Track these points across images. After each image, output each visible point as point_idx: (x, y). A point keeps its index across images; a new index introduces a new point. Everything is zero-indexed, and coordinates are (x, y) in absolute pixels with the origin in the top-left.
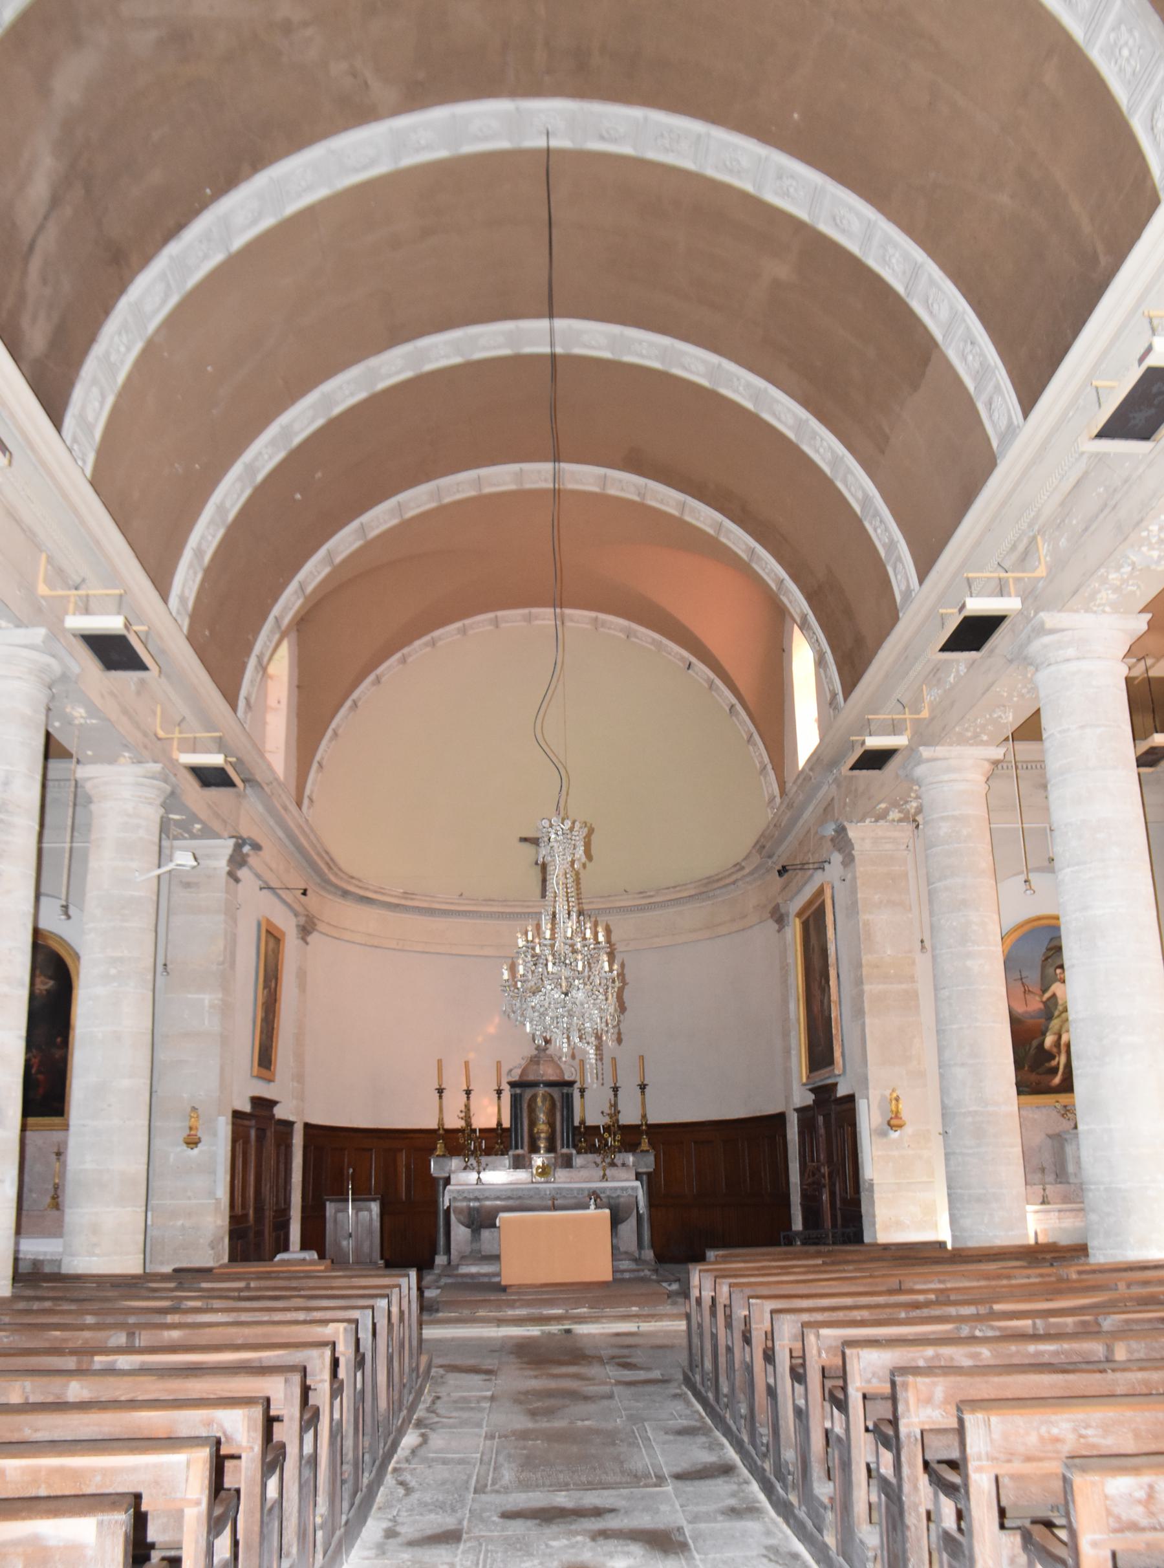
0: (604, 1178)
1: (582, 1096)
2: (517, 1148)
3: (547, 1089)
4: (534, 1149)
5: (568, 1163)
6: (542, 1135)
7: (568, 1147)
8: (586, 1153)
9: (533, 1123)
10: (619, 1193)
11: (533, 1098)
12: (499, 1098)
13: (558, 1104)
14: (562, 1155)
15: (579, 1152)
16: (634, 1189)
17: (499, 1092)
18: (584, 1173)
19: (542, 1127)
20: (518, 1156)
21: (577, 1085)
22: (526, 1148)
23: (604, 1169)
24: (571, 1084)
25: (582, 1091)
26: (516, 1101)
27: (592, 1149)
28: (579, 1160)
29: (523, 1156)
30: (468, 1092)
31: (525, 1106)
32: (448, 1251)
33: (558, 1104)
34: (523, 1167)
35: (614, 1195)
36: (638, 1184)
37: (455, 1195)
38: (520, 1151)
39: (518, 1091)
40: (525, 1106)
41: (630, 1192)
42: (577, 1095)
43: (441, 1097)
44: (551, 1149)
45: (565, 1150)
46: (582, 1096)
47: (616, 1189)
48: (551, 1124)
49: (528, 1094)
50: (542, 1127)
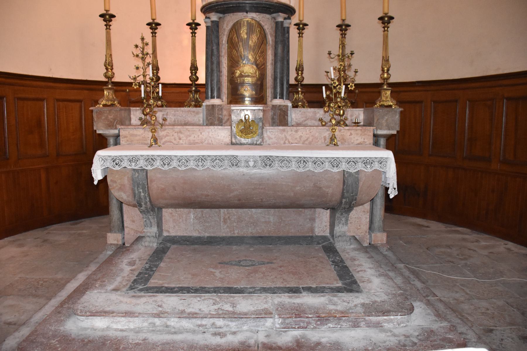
0: (333, 142)
1: (301, 35)
2: (212, 97)
3: (254, 15)
4: (236, 98)
5: (281, 119)
6: (248, 80)
7: (282, 97)
8: (303, 107)
9: (234, 63)
10: (360, 167)
11: (236, 28)
12: (194, 34)
13: (270, 39)
14: (274, 107)
15: (295, 106)
16: (382, 161)
17: (193, 26)
18: (303, 132)
19: (248, 68)
20: (213, 106)
21: (295, 19)
22: (225, 97)
23: (333, 130)
24: (289, 11)
25: (301, 27)
26: (213, 31)
27: (319, 103)
28: (295, 115)
29: (220, 108)
30: (154, 26)
31: (224, 39)
32: (122, 228)
33: (270, 39)
34: (220, 123)
35: (352, 171)
36: (389, 155)
37: (109, 164)
38: (216, 101)
39: (214, 17)
40: (224, 39)
41: (376, 166)
42: (294, 32)
43: (108, 26)
44: (259, 99)
45: (278, 102)
46: (301, 35)
47: (354, 161)
48: (261, 67)
49: (231, 19)
50: (248, 68)
